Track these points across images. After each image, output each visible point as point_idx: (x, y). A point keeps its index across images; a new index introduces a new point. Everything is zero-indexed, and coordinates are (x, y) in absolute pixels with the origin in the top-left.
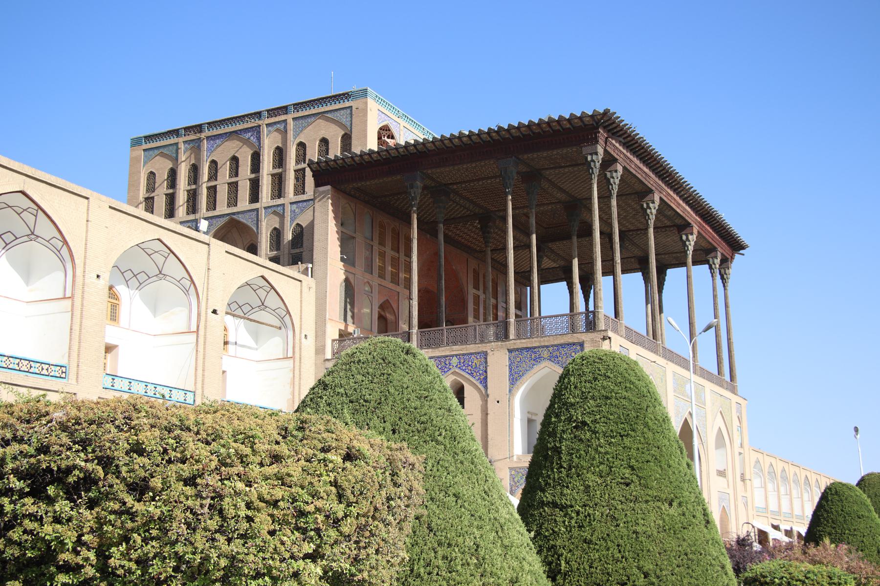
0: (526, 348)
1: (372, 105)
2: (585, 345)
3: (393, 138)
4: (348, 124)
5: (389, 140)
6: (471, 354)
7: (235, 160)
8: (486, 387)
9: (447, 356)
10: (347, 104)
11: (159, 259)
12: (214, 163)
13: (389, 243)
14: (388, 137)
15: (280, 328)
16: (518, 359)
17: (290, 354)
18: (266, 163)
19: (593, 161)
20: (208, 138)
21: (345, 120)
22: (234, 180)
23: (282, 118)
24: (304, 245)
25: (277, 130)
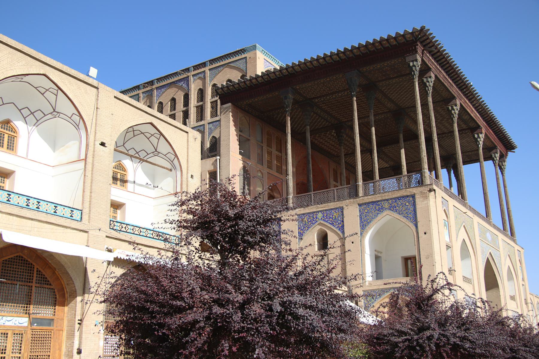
0: (372, 202)
2: (416, 196)
4: (245, 68)
6: (332, 209)
7: (173, 100)
8: (343, 232)
9: (314, 212)
10: (243, 56)
11: (52, 98)
12: (161, 103)
13: (274, 146)
15: (171, 170)
16: (366, 211)
18: (192, 99)
19: (414, 66)
20: (157, 88)
21: (242, 66)
22: (173, 112)
23: (203, 70)
25: (200, 78)
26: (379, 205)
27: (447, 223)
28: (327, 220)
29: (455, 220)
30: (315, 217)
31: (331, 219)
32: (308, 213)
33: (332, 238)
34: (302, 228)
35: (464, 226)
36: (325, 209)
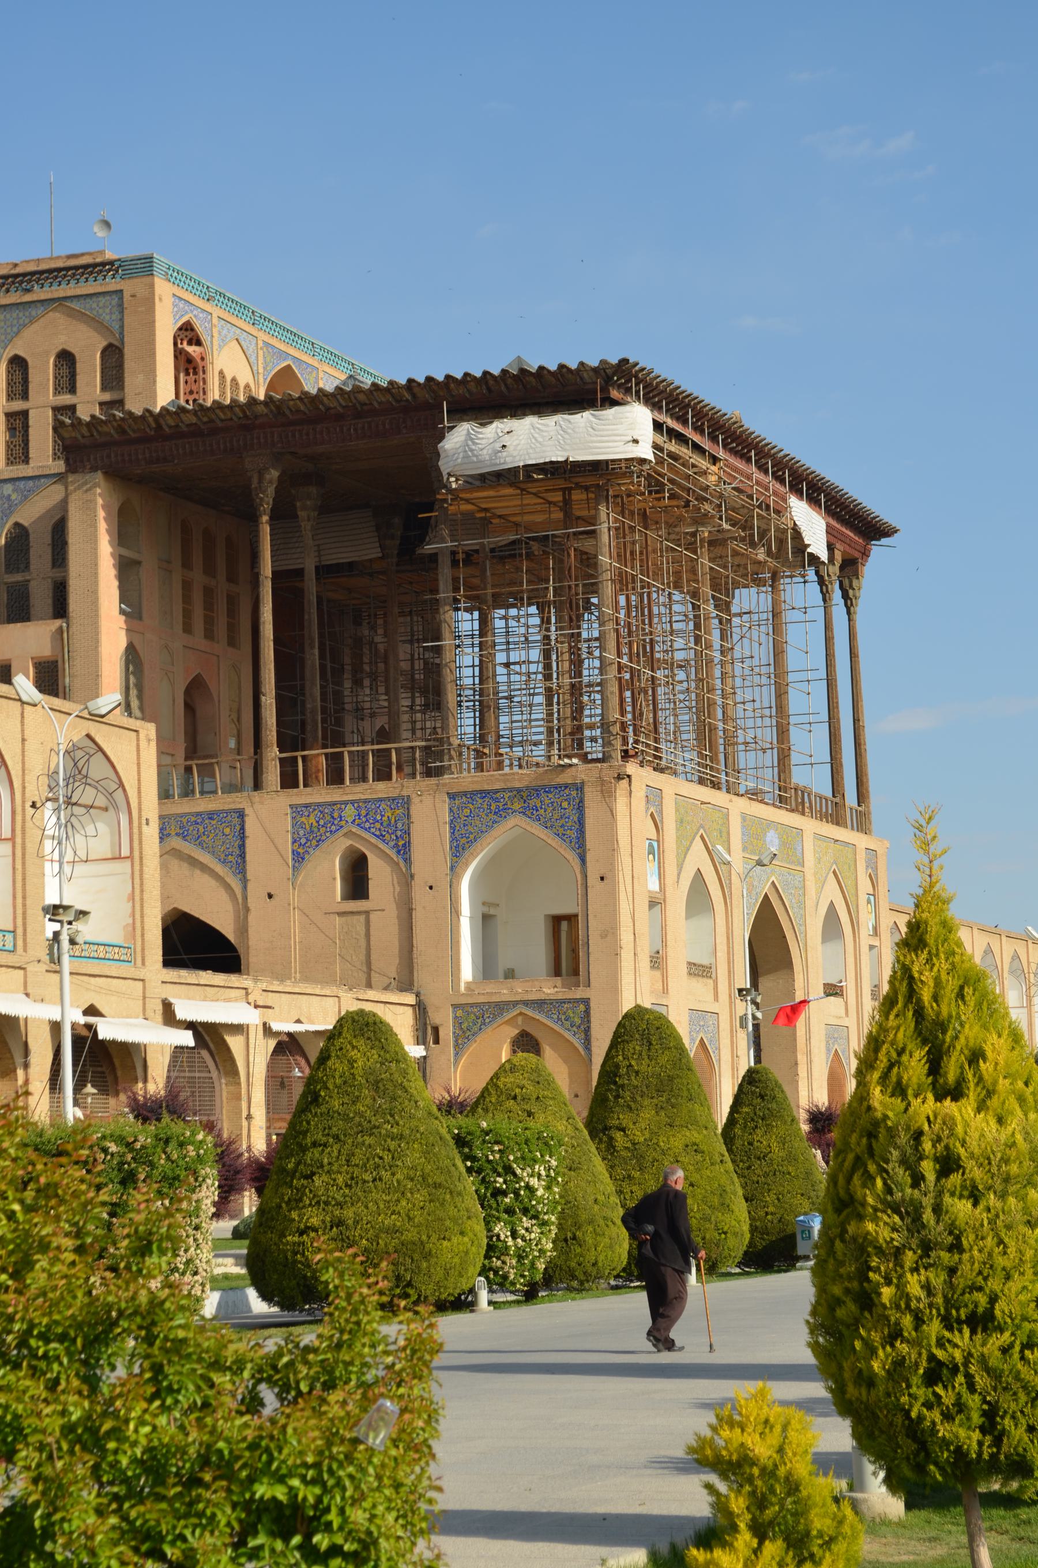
0: (481, 792)
1: (163, 288)
2: (586, 789)
3: (199, 343)
4: (116, 326)
5: (191, 349)
6: (381, 800)
8: (408, 861)
9: (334, 804)
10: (111, 284)
13: (197, 559)
14: (190, 343)
15: (106, 809)
16: (467, 812)
17: (125, 852)
21: (108, 317)
24: (32, 567)
26: (497, 800)
27: (655, 844)
28: (367, 825)
29: (678, 830)
30: (336, 815)
31: (378, 825)
32: (319, 805)
33: (379, 872)
34: (303, 841)
35: (702, 837)
36: (363, 797)
